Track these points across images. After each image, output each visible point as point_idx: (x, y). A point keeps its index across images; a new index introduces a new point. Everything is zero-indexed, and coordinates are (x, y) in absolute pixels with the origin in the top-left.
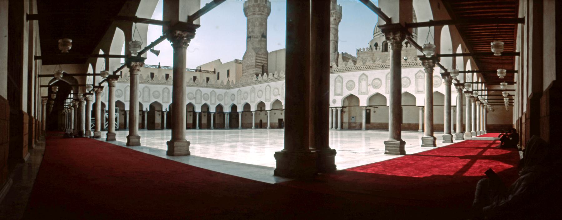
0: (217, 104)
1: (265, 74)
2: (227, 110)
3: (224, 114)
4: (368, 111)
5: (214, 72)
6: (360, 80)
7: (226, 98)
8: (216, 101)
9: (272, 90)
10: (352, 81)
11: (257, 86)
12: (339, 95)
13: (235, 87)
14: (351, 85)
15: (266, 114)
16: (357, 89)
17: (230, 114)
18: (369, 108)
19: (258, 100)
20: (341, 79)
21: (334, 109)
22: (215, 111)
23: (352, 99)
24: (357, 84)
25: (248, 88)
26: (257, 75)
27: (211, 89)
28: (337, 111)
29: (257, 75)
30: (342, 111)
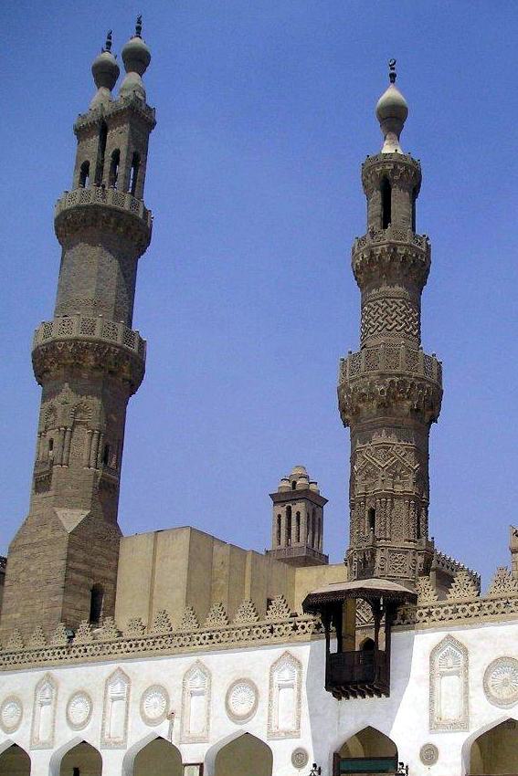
26: (72, 630)
29: (72, 630)
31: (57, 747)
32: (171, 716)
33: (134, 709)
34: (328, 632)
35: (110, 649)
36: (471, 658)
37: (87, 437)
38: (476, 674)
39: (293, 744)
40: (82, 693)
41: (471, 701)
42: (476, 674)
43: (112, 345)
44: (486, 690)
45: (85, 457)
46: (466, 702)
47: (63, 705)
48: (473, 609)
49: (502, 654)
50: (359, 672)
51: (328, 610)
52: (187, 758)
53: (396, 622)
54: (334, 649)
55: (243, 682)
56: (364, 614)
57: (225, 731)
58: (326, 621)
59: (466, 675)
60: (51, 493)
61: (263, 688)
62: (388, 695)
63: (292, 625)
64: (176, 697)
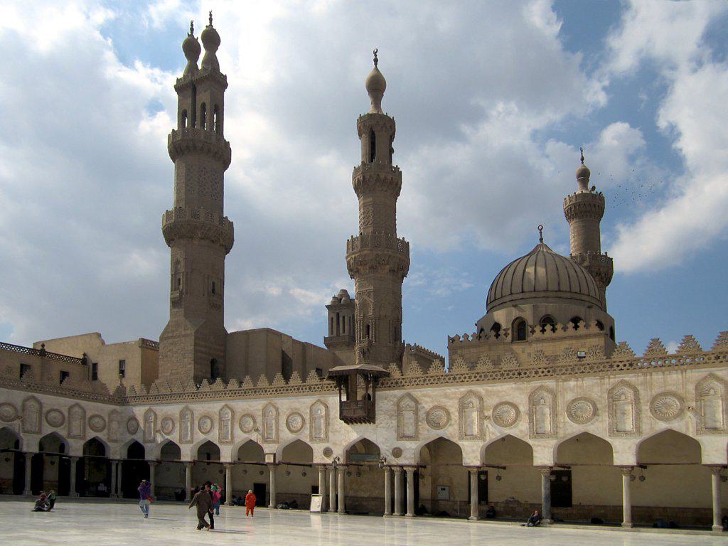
0: (88, 439)
1: (219, 380)
2: (117, 452)
3: (108, 462)
4: (483, 477)
5: (84, 361)
6: (463, 407)
7: (114, 425)
8: (84, 431)
9: (238, 417)
11: (199, 408)
12: (410, 438)
13: (139, 399)
15: (221, 472)
16: (456, 427)
17: (125, 464)
18: (486, 469)
19: (200, 438)
20: (413, 404)
21: (397, 470)
22: (80, 454)
23: (441, 449)
25: (173, 409)
27: (72, 401)
28: (404, 473)
30: (416, 475)
31: (195, 443)
34: (340, 390)
36: (419, 406)
39: (324, 445)
40: (207, 416)
46: (417, 428)
48: (420, 381)
49: (436, 404)
50: (360, 411)
51: (343, 381)
52: (266, 451)
54: (344, 398)
55: (295, 413)
56: (361, 381)
57: (287, 436)
58: (339, 385)
59: (417, 414)
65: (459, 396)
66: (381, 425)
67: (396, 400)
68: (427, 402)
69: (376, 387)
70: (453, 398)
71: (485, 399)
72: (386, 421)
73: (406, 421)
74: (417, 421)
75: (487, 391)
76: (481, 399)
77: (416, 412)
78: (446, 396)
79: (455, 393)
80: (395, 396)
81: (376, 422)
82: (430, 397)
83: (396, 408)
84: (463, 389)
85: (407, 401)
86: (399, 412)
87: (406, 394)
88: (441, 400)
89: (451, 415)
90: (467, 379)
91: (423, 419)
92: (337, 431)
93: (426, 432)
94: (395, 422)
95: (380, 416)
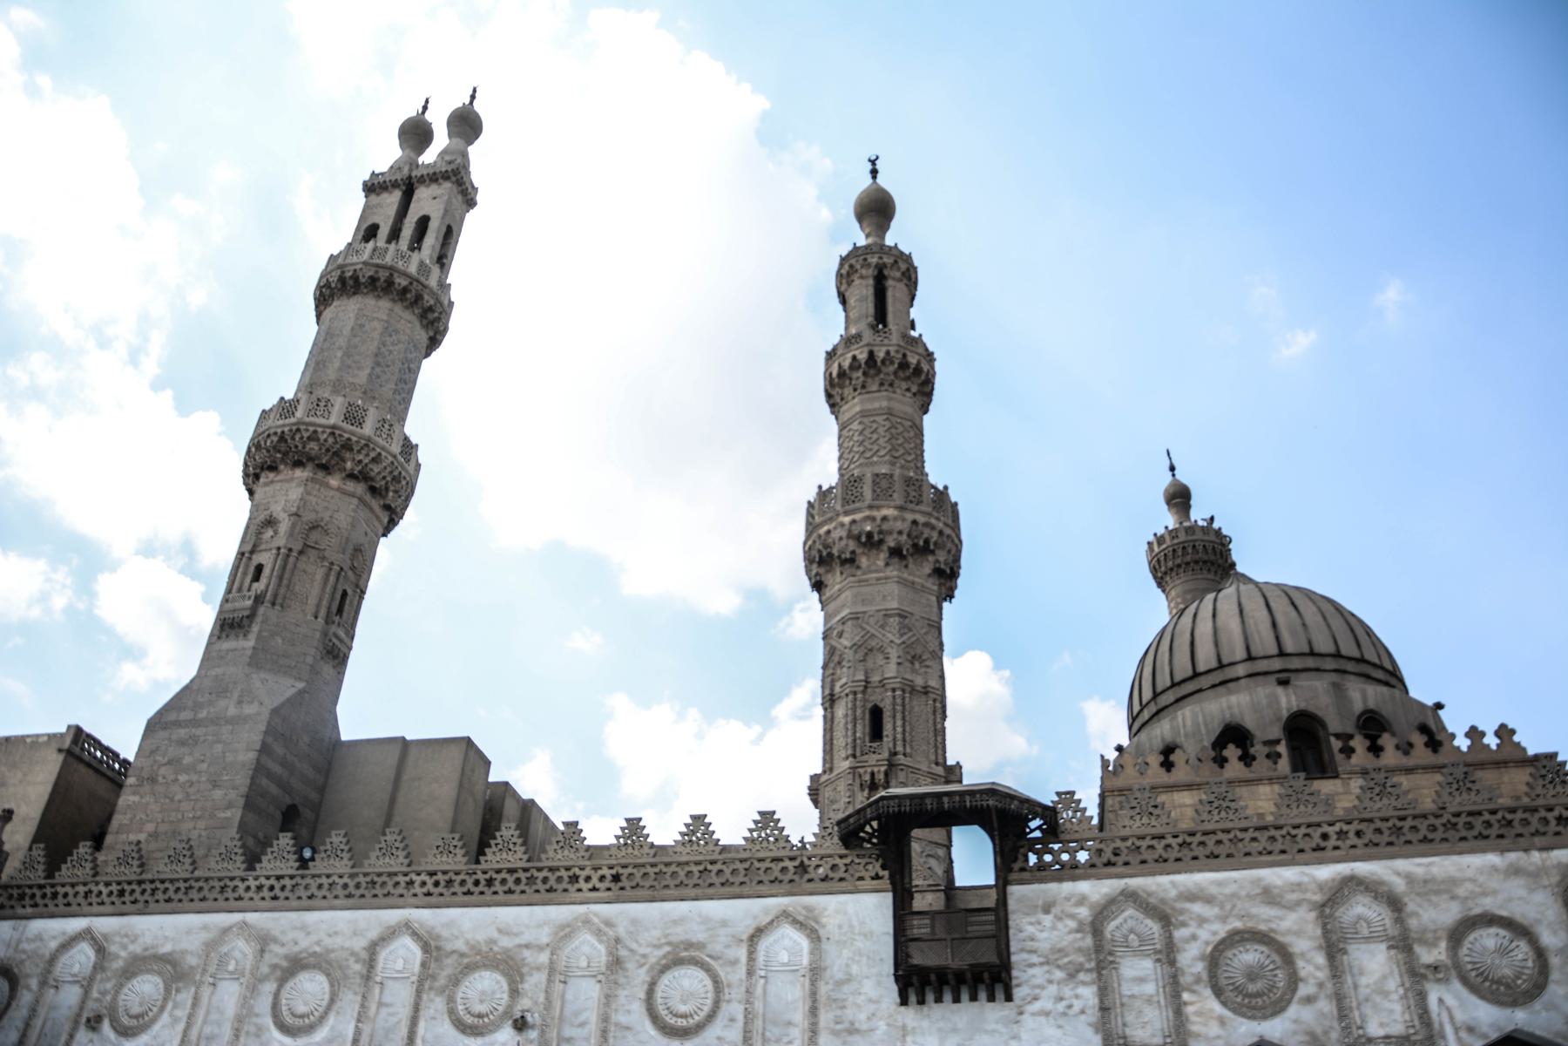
10: (1263, 938)
14: (1252, 976)
16: (1326, 1006)
20: (1153, 927)
24: (1312, 966)
32: (521, 1025)
33: (435, 1005)
35: (389, 887)
36: (1180, 934)
37: (320, 574)
38: (1191, 959)
41: (1190, 1010)
42: (1191, 959)
43: (383, 448)
44: (1218, 992)
45: (312, 601)
47: (269, 987)
49: (1238, 924)
53: (1016, 866)
60: (250, 642)
61: (735, 976)
62: (1009, 998)
63: (797, 863)
64: (534, 983)
65: (1318, 898)
66: (1037, 1006)
67: (1084, 912)
68: (1202, 921)
69: (1011, 870)
70: (1298, 903)
71: (1411, 907)
72: (1053, 989)
73: (1127, 990)
74: (1174, 987)
75: (1410, 879)
76: (1394, 903)
77: (1168, 954)
78: (1269, 896)
79: (1298, 887)
80: (1082, 900)
81: (1018, 993)
82: (1209, 900)
83: (1089, 941)
84: (1326, 872)
85: (1127, 920)
86: (1101, 960)
87: (1122, 893)
88: (1254, 911)
89: (1300, 963)
90: (1333, 842)
91: (1198, 980)
92: (857, 1031)
93: (1214, 1029)
94: (1088, 994)
95: (1028, 974)
